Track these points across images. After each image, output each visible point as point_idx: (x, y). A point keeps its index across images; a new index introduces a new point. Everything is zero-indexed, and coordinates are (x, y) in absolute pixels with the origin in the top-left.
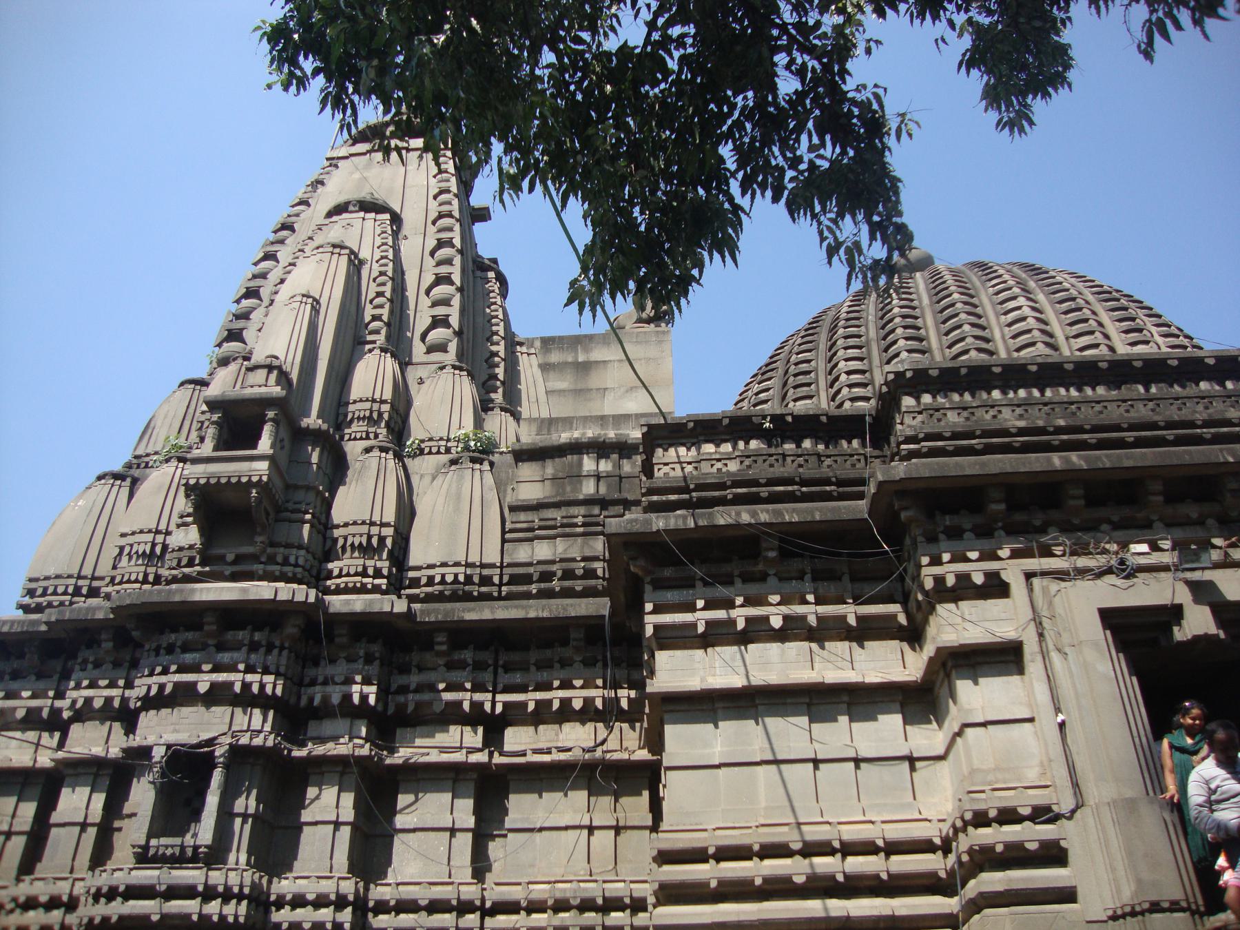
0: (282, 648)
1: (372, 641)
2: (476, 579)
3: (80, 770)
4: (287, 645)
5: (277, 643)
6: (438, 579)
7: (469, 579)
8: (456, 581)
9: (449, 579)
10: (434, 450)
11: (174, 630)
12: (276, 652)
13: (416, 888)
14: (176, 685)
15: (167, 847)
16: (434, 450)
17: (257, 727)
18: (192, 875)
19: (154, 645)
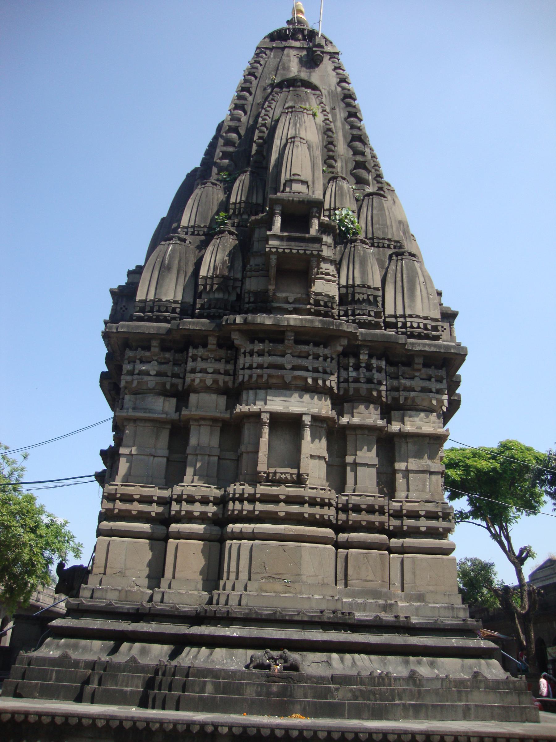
0: (332, 359)
1: (379, 358)
2: (429, 327)
3: (202, 422)
4: (334, 356)
5: (329, 355)
6: (409, 324)
7: (425, 325)
8: (419, 327)
9: (415, 325)
10: (381, 245)
11: (262, 341)
12: (329, 360)
13: (417, 504)
14: (269, 376)
15: (282, 473)
16: (381, 245)
17: (323, 407)
18: (283, 491)
19: (248, 350)
